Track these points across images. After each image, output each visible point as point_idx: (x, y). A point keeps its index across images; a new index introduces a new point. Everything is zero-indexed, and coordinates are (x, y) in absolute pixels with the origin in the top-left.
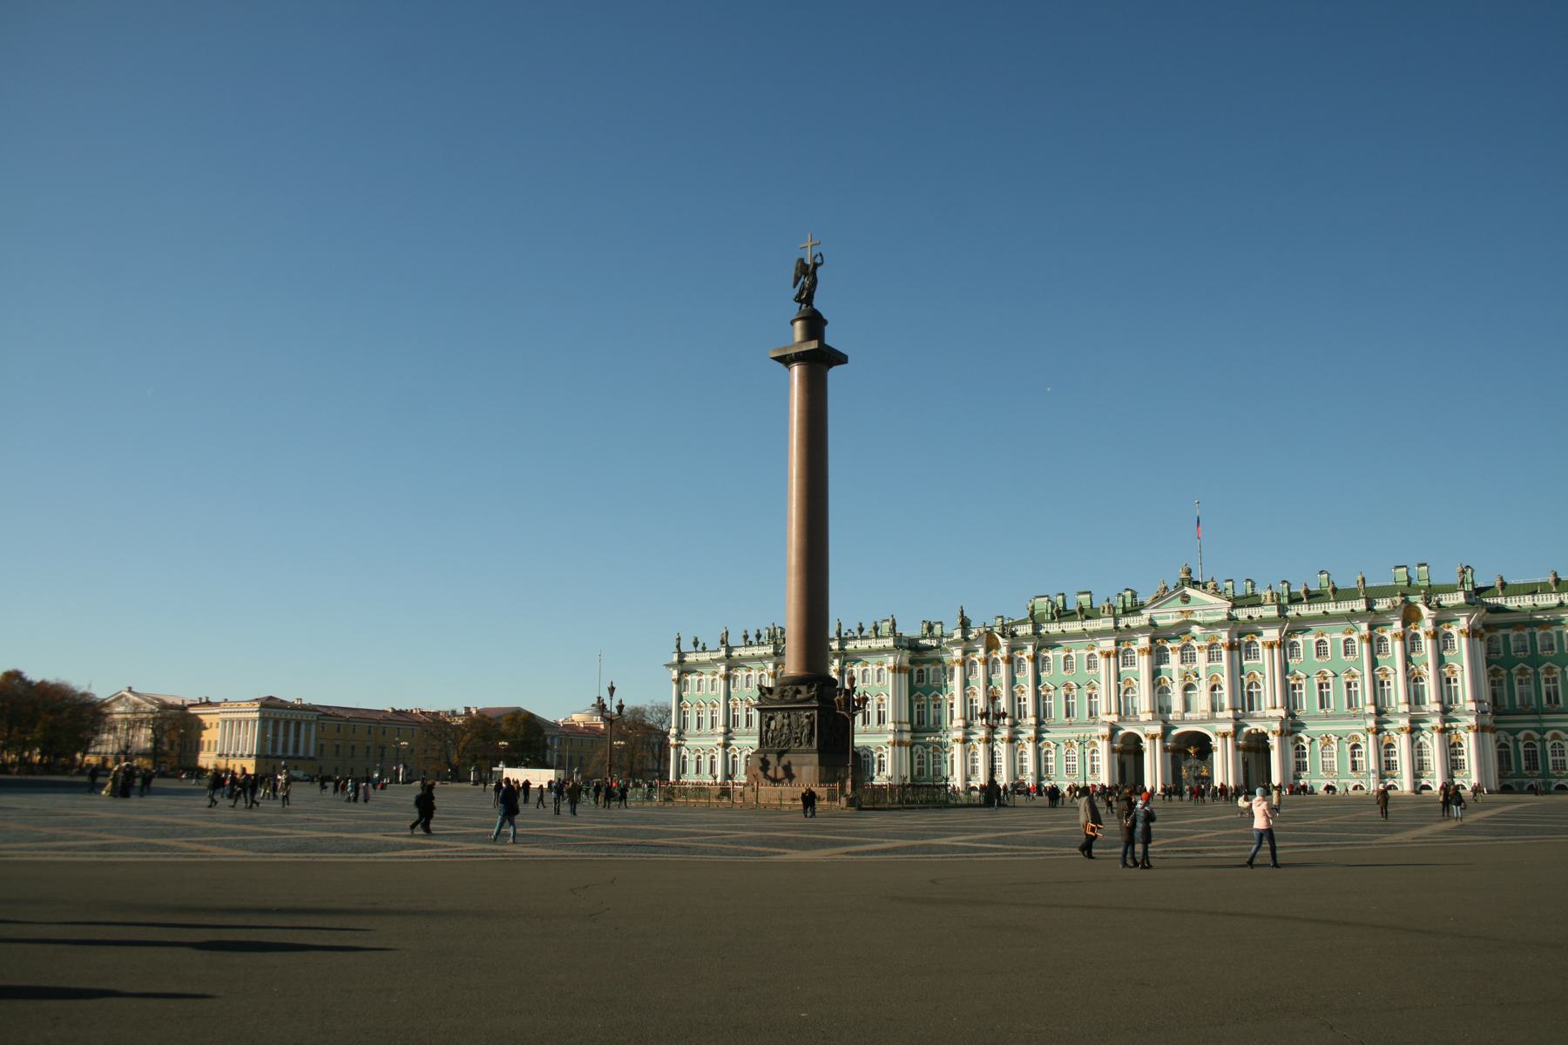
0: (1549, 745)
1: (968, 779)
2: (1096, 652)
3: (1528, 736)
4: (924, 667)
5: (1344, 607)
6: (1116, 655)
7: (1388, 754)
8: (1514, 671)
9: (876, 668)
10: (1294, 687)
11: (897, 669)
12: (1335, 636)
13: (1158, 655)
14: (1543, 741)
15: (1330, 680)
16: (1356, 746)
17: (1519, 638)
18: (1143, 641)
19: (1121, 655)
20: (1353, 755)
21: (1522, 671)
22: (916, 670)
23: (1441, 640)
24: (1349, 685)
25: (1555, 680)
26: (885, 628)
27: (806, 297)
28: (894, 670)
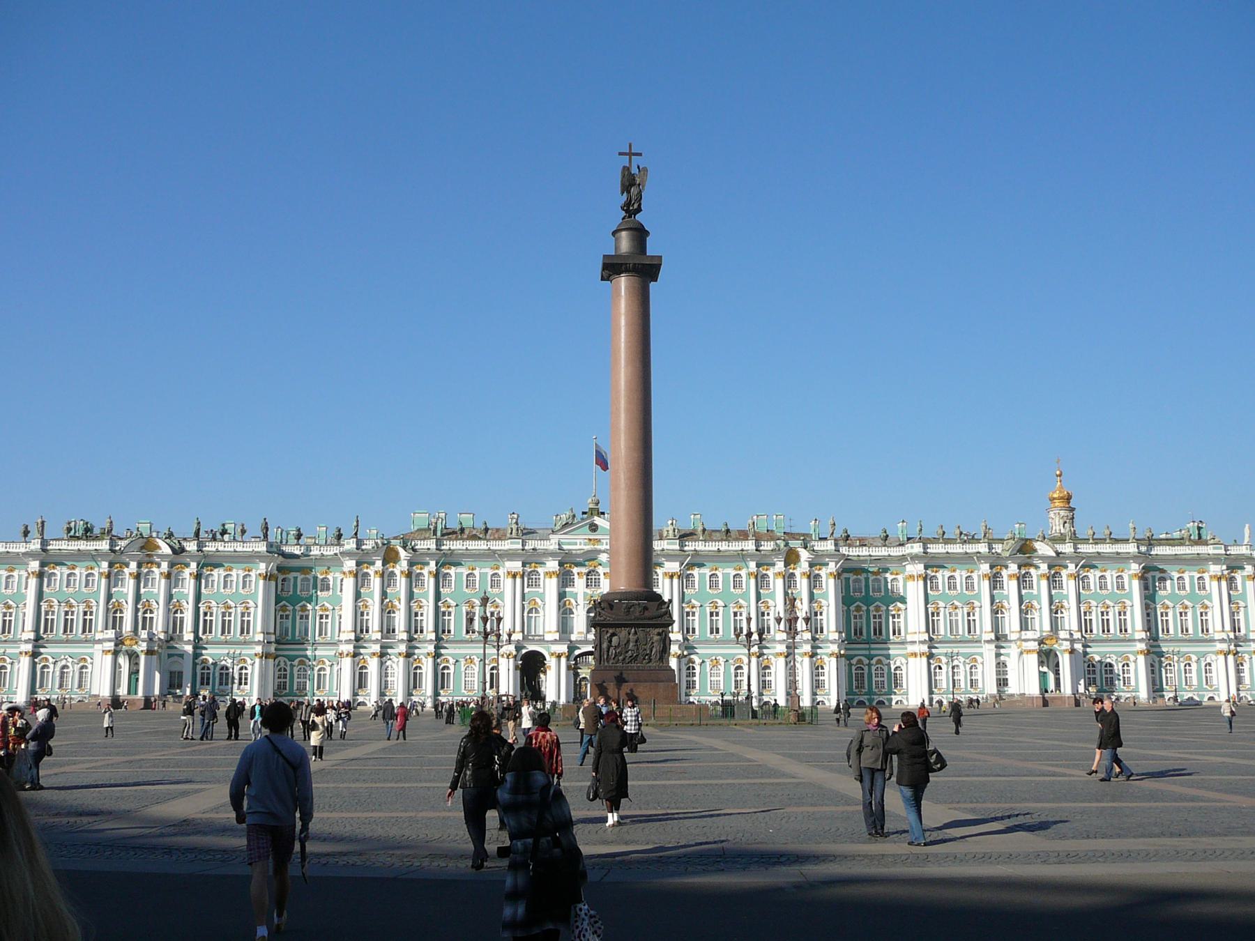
0: (873, 668)
1: (410, 694)
2: (501, 572)
3: (860, 662)
4: (291, 576)
5: (736, 546)
6: (522, 577)
7: (764, 675)
8: (852, 608)
9: (242, 574)
10: (416, 614)
11: (268, 577)
12: (483, 570)
13: (565, 579)
14: (869, 665)
15: (721, 610)
16: (739, 668)
17: (856, 581)
18: (553, 565)
19: (528, 577)
20: (736, 676)
21: (858, 609)
22: (281, 577)
23: (814, 580)
24: (735, 614)
25: (880, 616)
26: (255, 529)
27: (631, 209)
28: (265, 578)
